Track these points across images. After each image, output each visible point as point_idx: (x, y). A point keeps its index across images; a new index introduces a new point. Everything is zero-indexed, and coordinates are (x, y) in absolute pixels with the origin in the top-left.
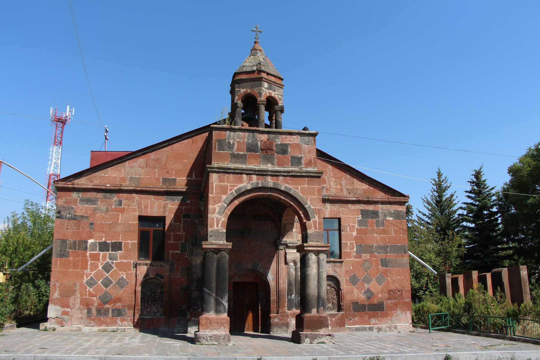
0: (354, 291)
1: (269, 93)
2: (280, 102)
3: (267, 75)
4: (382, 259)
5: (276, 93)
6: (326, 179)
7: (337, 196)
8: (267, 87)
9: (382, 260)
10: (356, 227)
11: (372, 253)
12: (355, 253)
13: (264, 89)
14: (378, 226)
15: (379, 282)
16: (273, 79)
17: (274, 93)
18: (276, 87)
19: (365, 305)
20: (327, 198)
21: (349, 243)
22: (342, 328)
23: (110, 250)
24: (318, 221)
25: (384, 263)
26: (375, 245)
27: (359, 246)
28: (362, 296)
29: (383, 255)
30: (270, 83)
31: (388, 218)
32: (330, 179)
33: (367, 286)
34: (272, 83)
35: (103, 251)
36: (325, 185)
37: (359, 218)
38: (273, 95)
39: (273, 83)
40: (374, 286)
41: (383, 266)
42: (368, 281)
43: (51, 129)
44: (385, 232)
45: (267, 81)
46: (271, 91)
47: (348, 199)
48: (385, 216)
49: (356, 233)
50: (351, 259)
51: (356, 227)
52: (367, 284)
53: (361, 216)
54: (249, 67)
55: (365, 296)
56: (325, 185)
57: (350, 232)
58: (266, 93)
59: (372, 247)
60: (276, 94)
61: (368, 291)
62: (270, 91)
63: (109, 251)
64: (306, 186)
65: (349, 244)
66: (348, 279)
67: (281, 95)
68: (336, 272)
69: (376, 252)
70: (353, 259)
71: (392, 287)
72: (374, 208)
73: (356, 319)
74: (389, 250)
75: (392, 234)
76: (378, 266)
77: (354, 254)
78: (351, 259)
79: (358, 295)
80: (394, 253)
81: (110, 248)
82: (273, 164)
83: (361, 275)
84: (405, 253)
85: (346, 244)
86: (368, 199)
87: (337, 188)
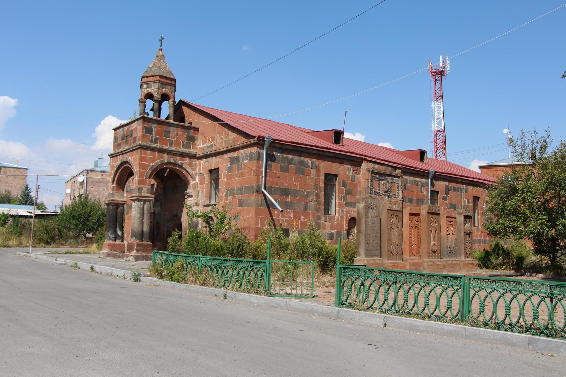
2: (155, 94)
10: (227, 174)
14: (238, 171)
21: (222, 188)
26: (236, 187)
29: (238, 197)
30: (147, 83)
31: (245, 162)
37: (228, 165)
38: (150, 92)
41: (239, 207)
43: (429, 83)
45: (145, 83)
47: (221, 150)
48: (243, 161)
49: (226, 179)
51: (227, 174)
53: (229, 163)
56: (214, 142)
59: (234, 190)
64: (135, 156)
72: (237, 154)
76: (236, 206)
80: (246, 194)
82: (128, 145)
84: (253, 193)
85: (221, 189)
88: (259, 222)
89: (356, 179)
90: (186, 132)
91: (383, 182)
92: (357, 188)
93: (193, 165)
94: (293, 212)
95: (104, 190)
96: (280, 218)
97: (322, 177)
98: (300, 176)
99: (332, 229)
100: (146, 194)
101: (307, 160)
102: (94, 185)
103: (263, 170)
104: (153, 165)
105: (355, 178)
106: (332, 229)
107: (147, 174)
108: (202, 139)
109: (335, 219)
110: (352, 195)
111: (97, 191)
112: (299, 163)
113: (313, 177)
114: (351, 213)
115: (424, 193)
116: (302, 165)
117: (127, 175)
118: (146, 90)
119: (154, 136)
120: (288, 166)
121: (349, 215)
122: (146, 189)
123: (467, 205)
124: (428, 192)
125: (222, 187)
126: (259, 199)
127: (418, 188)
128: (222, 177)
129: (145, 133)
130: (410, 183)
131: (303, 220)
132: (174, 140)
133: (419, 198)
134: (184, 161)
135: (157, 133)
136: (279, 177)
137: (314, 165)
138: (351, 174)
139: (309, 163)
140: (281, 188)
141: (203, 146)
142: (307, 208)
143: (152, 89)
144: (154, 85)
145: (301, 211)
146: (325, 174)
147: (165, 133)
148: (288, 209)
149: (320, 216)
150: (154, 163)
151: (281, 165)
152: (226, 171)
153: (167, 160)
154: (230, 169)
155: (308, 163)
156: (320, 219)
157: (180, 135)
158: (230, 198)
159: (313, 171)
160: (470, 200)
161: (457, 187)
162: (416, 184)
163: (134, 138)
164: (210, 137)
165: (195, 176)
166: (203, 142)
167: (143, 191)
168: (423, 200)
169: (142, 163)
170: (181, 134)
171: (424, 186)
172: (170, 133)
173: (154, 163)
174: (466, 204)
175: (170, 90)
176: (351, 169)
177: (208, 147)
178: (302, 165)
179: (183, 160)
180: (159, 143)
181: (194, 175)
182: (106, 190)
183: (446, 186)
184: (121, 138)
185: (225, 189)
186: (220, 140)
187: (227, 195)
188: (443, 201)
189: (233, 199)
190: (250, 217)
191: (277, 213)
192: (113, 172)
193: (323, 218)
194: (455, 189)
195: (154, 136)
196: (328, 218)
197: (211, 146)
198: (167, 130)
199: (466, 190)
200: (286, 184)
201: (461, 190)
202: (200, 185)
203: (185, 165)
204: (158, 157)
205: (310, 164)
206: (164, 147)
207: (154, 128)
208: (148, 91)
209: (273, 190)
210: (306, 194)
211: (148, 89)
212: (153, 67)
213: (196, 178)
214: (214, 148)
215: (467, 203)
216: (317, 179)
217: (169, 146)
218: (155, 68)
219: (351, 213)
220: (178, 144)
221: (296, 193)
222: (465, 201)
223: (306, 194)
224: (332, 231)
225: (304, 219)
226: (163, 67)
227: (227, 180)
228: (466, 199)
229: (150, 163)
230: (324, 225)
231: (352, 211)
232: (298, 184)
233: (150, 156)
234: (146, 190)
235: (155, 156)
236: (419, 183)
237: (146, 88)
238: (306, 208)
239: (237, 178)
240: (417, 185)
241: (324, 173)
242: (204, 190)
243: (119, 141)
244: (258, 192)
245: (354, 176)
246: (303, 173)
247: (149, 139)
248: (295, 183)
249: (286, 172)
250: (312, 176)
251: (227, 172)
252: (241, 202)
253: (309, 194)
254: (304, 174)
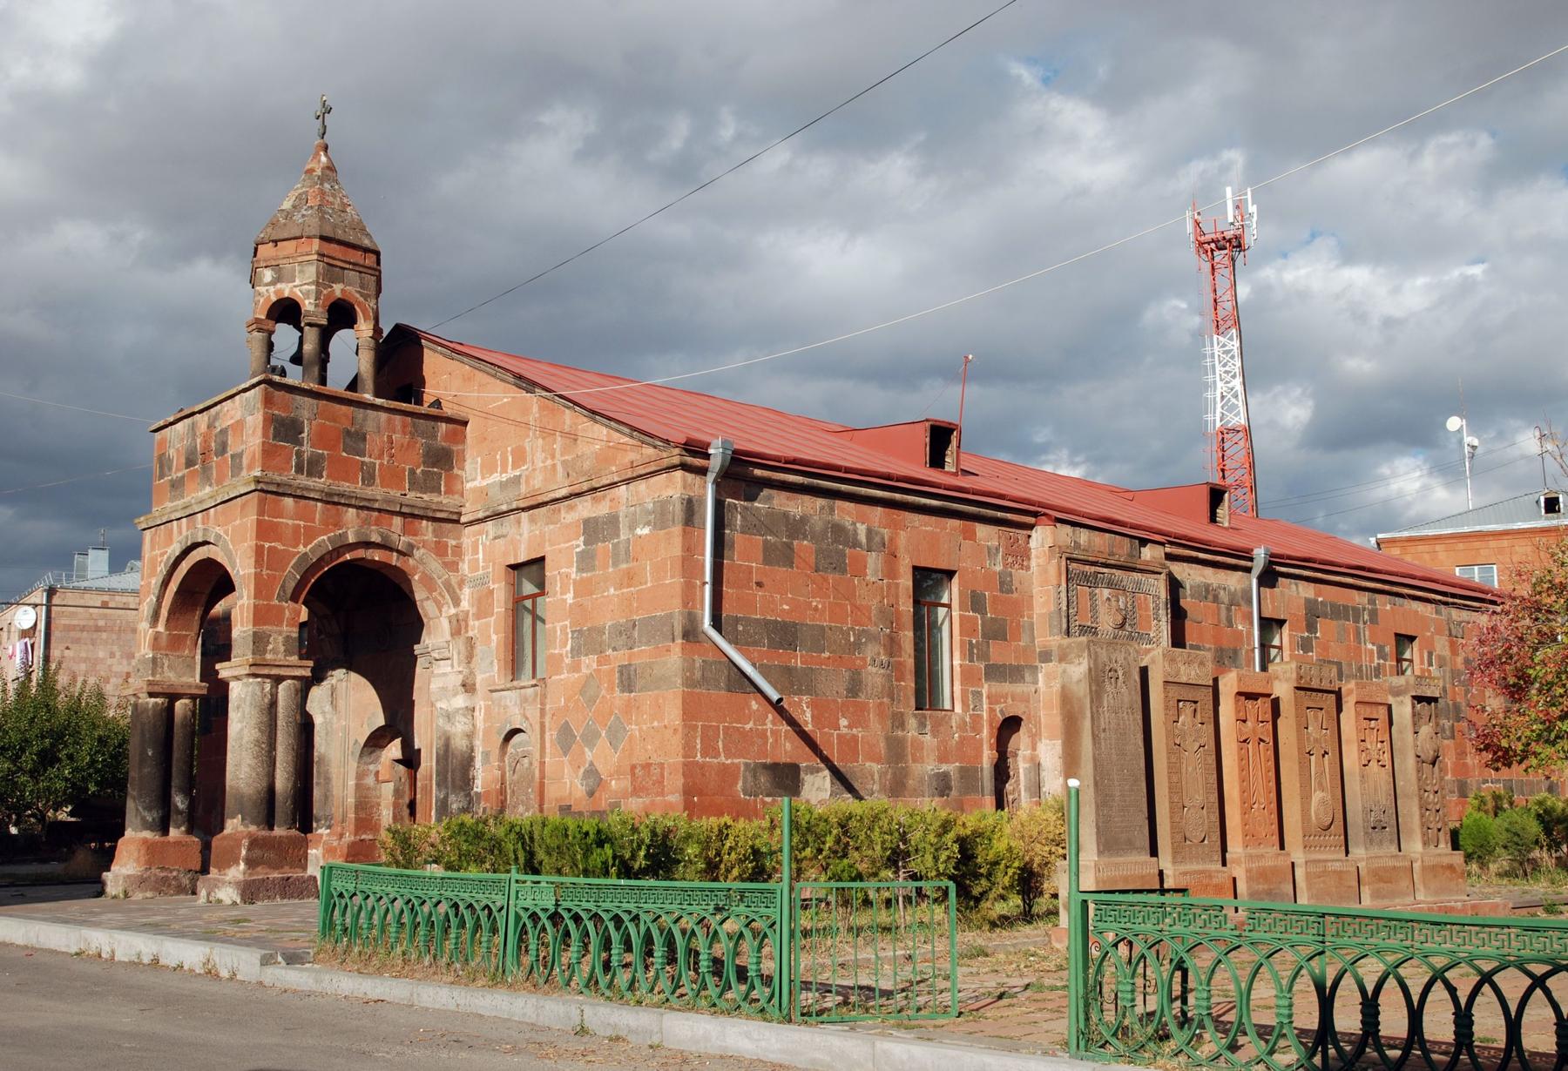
2: (307, 302)
12: (570, 655)
14: (615, 564)
26: (610, 623)
28: (579, 786)
31: (639, 531)
33: (589, 755)
37: (578, 546)
38: (286, 295)
40: (602, 756)
41: (623, 691)
42: (590, 738)
48: (632, 528)
50: (562, 677)
53: (582, 538)
57: (561, 594)
59: (601, 631)
64: (238, 522)
65: (559, 632)
71: (639, 758)
72: (611, 507)
78: (562, 677)
80: (648, 643)
88: (698, 741)
89: (1016, 584)
90: (422, 435)
91: (1106, 592)
92: (1022, 616)
93: (450, 552)
94: (812, 705)
95: (112, 655)
96: (769, 726)
97: (906, 582)
98: (832, 577)
99: (943, 759)
100: (281, 656)
101: (854, 524)
102: (77, 641)
103: (704, 560)
104: (306, 553)
105: (1011, 581)
106: (943, 759)
107: (283, 586)
108: (479, 459)
109: (954, 724)
110: (1006, 640)
111: (85, 660)
112: (824, 531)
113: (873, 579)
114: (1005, 702)
115: (1240, 627)
116: (836, 541)
117: (208, 591)
118: (272, 289)
119: (307, 449)
120: (789, 546)
121: (997, 708)
122: (280, 639)
123: (1379, 664)
124: (1251, 623)
125: (558, 626)
126: (694, 660)
127: (1219, 609)
128: (558, 589)
129: (275, 438)
130: (1192, 596)
131: (845, 731)
132: (381, 465)
133: (1225, 645)
134: (418, 538)
135: (321, 439)
136: (759, 584)
137: (877, 539)
138: (999, 568)
139: (859, 532)
140: (767, 622)
141: (485, 483)
142: (859, 690)
143: (295, 286)
144: (301, 272)
145: (839, 700)
146: (915, 568)
147: (348, 440)
148: (795, 694)
149: (902, 714)
150: (309, 547)
151: (765, 542)
152: (570, 566)
153: (357, 533)
154: (586, 561)
155: (855, 530)
156: (902, 725)
157: (402, 446)
158: (589, 662)
159: (874, 561)
160: (1387, 649)
161: (1344, 606)
162: (1210, 597)
163: (232, 456)
164: (509, 449)
165: (458, 591)
166: (482, 466)
167: (270, 647)
168: (1235, 652)
169: (267, 545)
170: (405, 444)
171: (1239, 605)
172: (364, 439)
173: (309, 547)
174: (1376, 661)
175: (361, 287)
176: (997, 549)
177: (503, 486)
178: (836, 541)
179: (415, 535)
180: (324, 474)
181: (456, 586)
182: (118, 654)
183: (1307, 601)
184: (183, 460)
185: (569, 630)
186: (546, 458)
187: (576, 652)
188: (1301, 652)
189: (600, 663)
190: (665, 727)
191: (758, 710)
192: (153, 582)
193: (912, 723)
194: (1339, 612)
195: (307, 449)
196: (928, 723)
197: (516, 481)
198: (353, 430)
199: (1374, 614)
200: (786, 607)
201: (1357, 614)
202: (478, 619)
203: (422, 551)
204: (325, 522)
205: (862, 538)
206: (345, 486)
207: (306, 421)
208: (281, 291)
209: (740, 628)
210: (852, 639)
211: (279, 286)
212: (294, 207)
213: (462, 597)
214: (523, 489)
215: (1379, 659)
216: (889, 586)
217: (363, 483)
218: (305, 213)
219: (1005, 702)
220: (393, 477)
221: (819, 638)
222: (1371, 652)
223: (852, 639)
224: (944, 768)
225: (850, 727)
226: (333, 209)
227: (574, 598)
228: (1373, 644)
229: (296, 546)
230: (919, 746)
231: (1007, 694)
232: (824, 606)
233: (296, 522)
234: (281, 644)
235: (313, 522)
236: (1222, 592)
237: (273, 283)
238: (855, 688)
239: (612, 591)
240: (1216, 599)
241: (911, 565)
242: (490, 636)
243: (178, 470)
244: (691, 638)
245: (1011, 575)
246: (839, 568)
247: (291, 458)
248: (814, 604)
249: (784, 566)
250: (870, 578)
251: (574, 569)
252: (629, 675)
253: (864, 640)
254: (844, 571)
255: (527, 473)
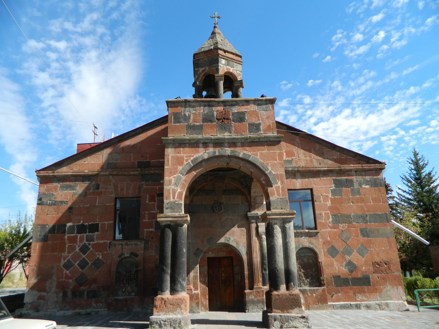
0: (333, 264)
1: (227, 69)
3: (225, 53)
4: (362, 229)
5: (235, 69)
6: (295, 152)
7: (307, 167)
8: (224, 63)
9: (362, 230)
10: (330, 197)
11: (350, 223)
13: (222, 66)
14: (353, 195)
15: (361, 253)
16: (231, 56)
17: (232, 69)
18: (235, 64)
19: (348, 279)
20: (296, 169)
22: (325, 305)
23: (88, 232)
24: (280, 187)
25: (365, 233)
26: (353, 214)
27: (335, 216)
28: (344, 269)
29: (363, 225)
30: (227, 60)
31: (364, 186)
32: (299, 152)
33: (348, 258)
34: (229, 59)
35: (80, 234)
36: (294, 158)
37: (332, 187)
38: (231, 71)
39: (230, 60)
44: (362, 200)
46: (230, 67)
47: (319, 169)
49: (330, 202)
50: (328, 230)
51: (330, 197)
52: (348, 255)
53: (334, 185)
54: (207, 48)
55: (347, 269)
56: (294, 158)
57: (324, 202)
58: (224, 69)
60: (234, 70)
61: (350, 264)
62: (228, 67)
63: (86, 233)
65: (324, 215)
66: (326, 250)
67: (240, 71)
68: (312, 244)
69: (354, 222)
70: (330, 230)
71: (377, 259)
73: (340, 294)
74: (368, 219)
75: (370, 203)
76: (358, 236)
77: (330, 225)
78: (328, 230)
79: (339, 268)
81: (88, 230)
82: (230, 132)
83: (340, 246)
84: (388, 222)
86: (339, 168)
87: (307, 160)
158: (342, 226)
214: (294, 165)
239: (352, 204)
251: (330, 194)
255: (296, 160)
